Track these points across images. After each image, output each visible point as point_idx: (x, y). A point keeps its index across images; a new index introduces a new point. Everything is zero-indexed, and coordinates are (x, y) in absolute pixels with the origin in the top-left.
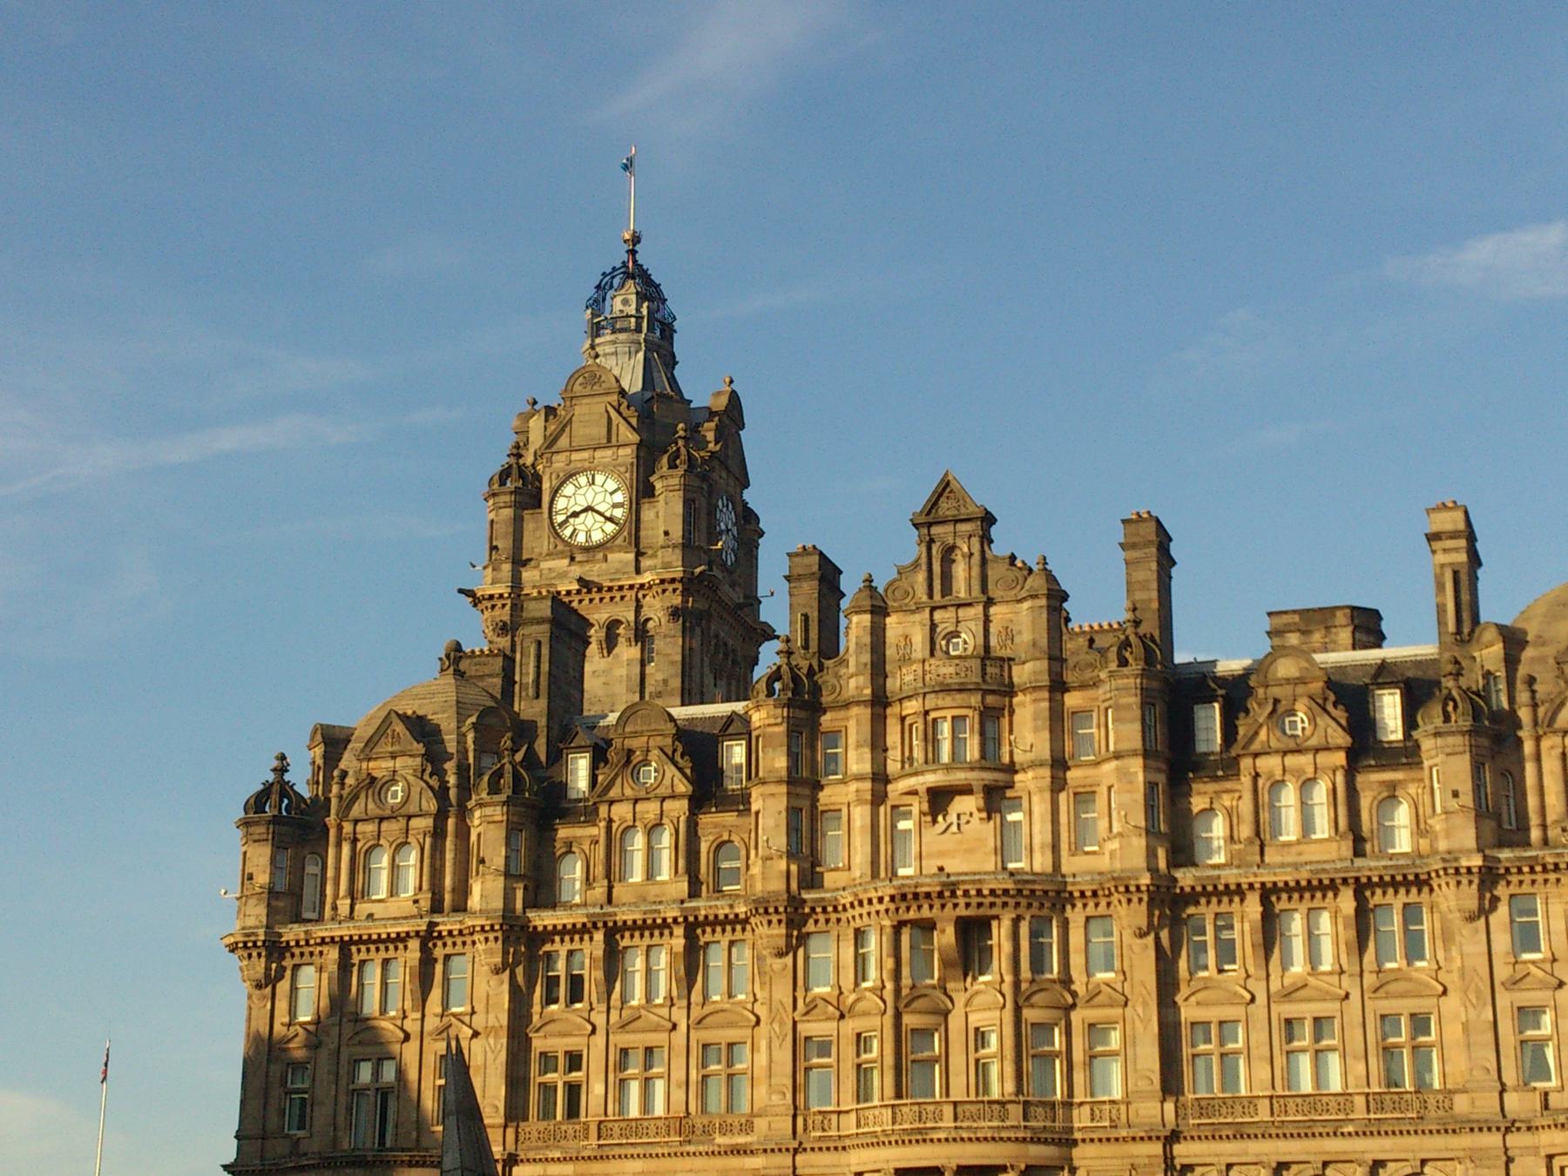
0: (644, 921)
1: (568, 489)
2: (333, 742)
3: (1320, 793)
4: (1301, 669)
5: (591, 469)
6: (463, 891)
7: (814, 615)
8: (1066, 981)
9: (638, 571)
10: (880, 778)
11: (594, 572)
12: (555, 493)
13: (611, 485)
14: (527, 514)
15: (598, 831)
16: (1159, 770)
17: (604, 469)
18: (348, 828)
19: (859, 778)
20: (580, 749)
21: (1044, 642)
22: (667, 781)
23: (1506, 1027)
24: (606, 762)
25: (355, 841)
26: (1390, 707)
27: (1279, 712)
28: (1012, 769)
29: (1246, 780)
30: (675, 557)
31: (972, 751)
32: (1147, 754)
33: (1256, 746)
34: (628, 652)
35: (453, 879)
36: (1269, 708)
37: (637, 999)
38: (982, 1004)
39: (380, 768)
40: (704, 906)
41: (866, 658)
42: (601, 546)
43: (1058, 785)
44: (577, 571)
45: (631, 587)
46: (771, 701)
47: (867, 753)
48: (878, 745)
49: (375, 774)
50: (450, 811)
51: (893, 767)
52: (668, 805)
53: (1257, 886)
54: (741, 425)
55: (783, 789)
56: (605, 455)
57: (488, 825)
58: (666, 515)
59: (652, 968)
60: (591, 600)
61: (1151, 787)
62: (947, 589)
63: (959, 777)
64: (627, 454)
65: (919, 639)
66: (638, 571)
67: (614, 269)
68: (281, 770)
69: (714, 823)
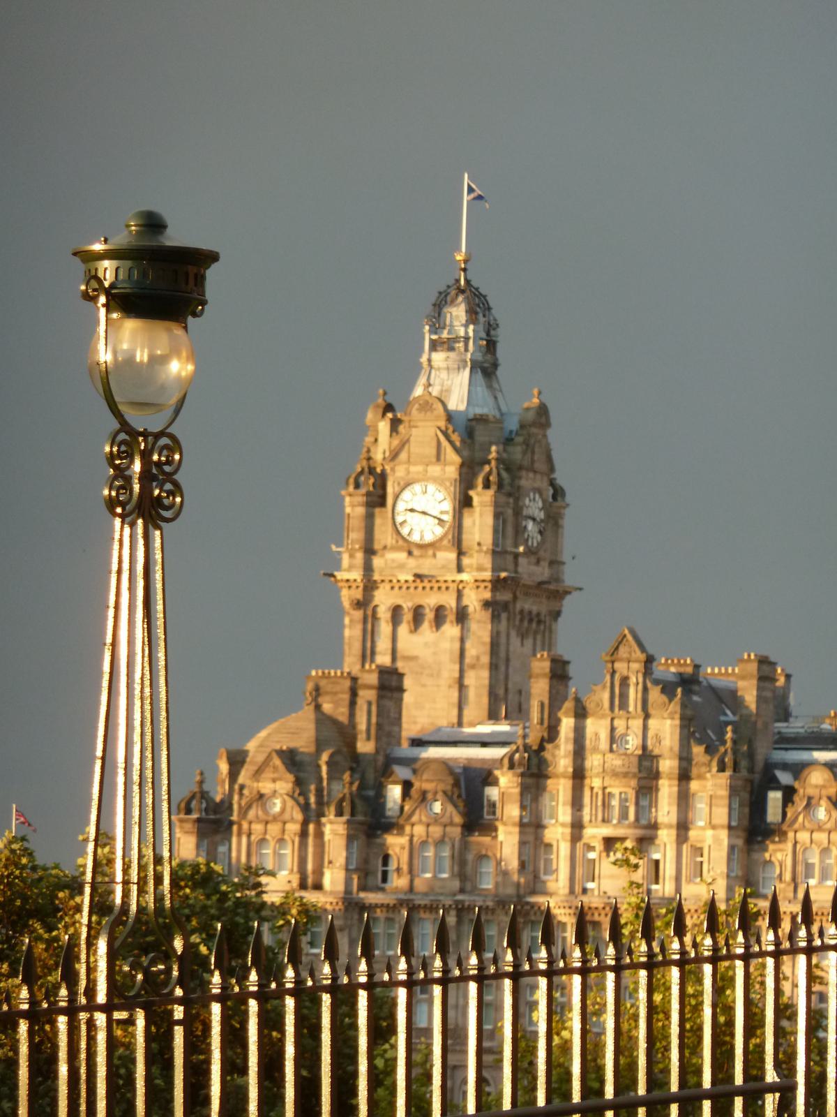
0: (432, 905)
1: (406, 495)
4: (825, 780)
5: (424, 478)
6: (319, 872)
7: (546, 702)
9: (460, 569)
10: (577, 827)
11: (426, 565)
12: (397, 497)
13: (441, 496)
14: (377, 510)
15: (404, 840)
16: (738, 837)
17: (435, 480)
18: (245, 826)
19: (563, 825)
20: (395, 783)
21: (676, 748)
22: (448, 814)
24: (410, 798)
25: (249, 835)
27: (810, 804)
29: (789, 845)
30: (487, 561)
32: (730, 828)
33: (796, 826)
34: (451, 629)
35: (314, 866)
36: (805, 803)
39: (266, 786)
41: (570, 747)
42: (431, 545)
44: (412, 562)
45: (453, 581)
46: (511, 772)
47: (569, 810)
48: (577, 804)
49: (263, 791)
51: (586, 818)
52: (448, 829)
53: (788, 913)
54: (547, 425)
55: (517, 830)
56: (435, 470)
58: (480, 524)
60: (424, 588)
61: (732, 848)
62: (624, 705)
63: (619, 832)
64: (452, 471)
65: (604, 735)
66: (460, 569)
67: (449, 287)
68: (201, 782)
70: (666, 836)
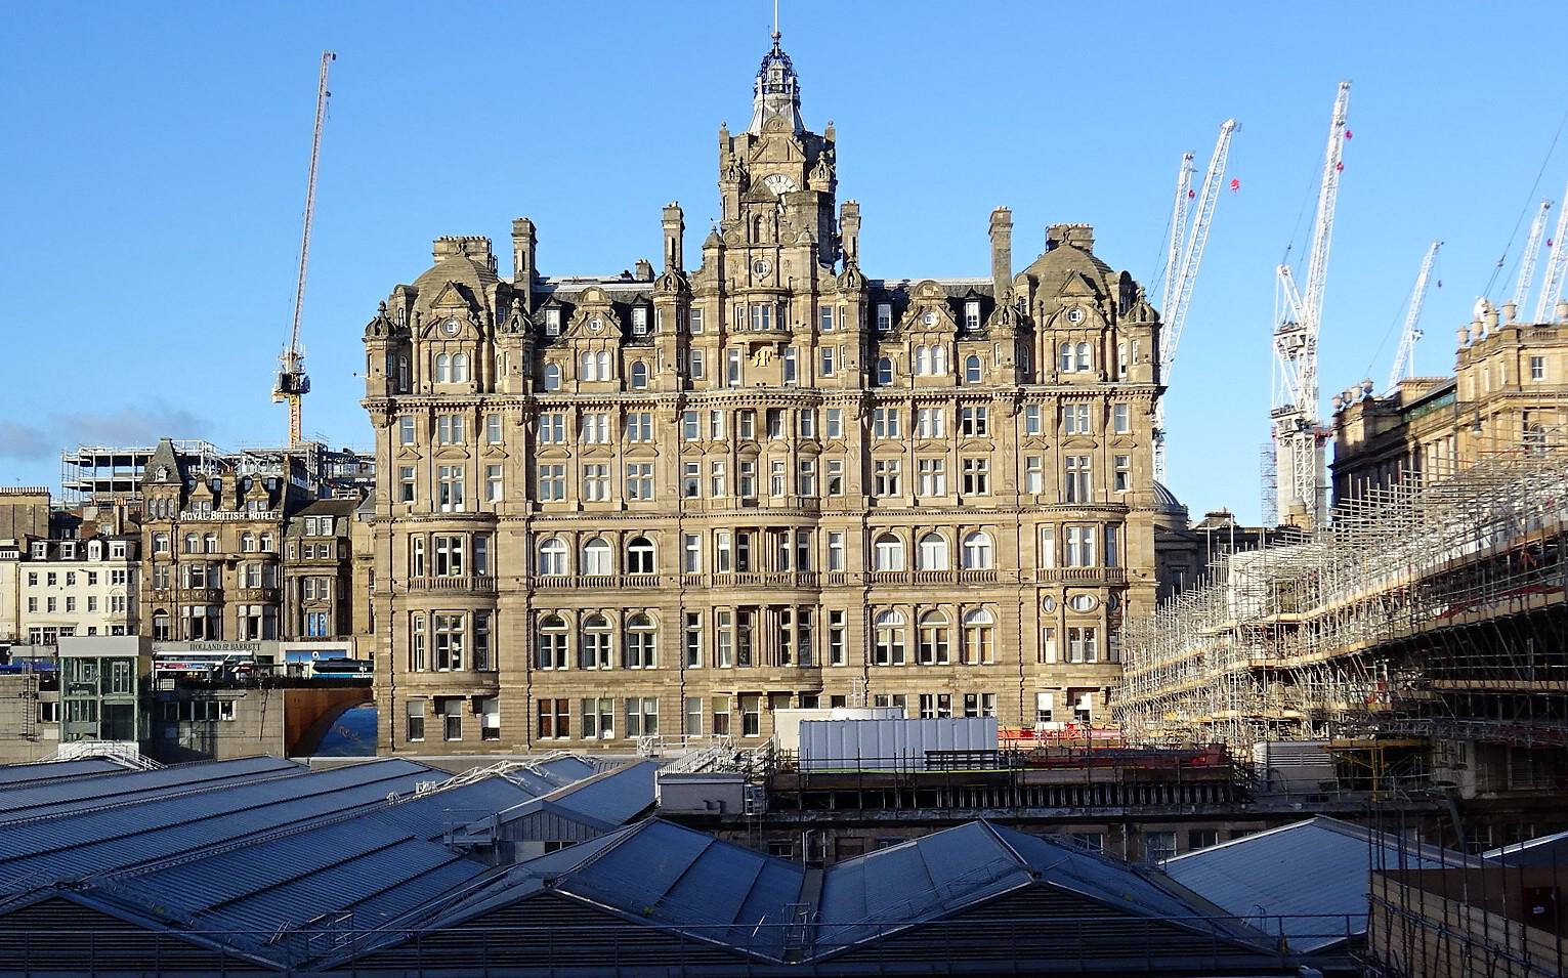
2: (411, 295)
3: (941, 353)
8: (818, 440)
10: (723, 335)
23: (1022, 466)
26: (973, 309)
28: (791, 334)
31: (773, 324)
37: (592, 440)
38: (777, 451)
39: (443, 312)
40: (629, 397)
43: (815, 343)
50: (485, 337)
57: (509, 349)
59: (602, 427)
62: (757, 239)
69: (631, 354)
70: (802, 339)
